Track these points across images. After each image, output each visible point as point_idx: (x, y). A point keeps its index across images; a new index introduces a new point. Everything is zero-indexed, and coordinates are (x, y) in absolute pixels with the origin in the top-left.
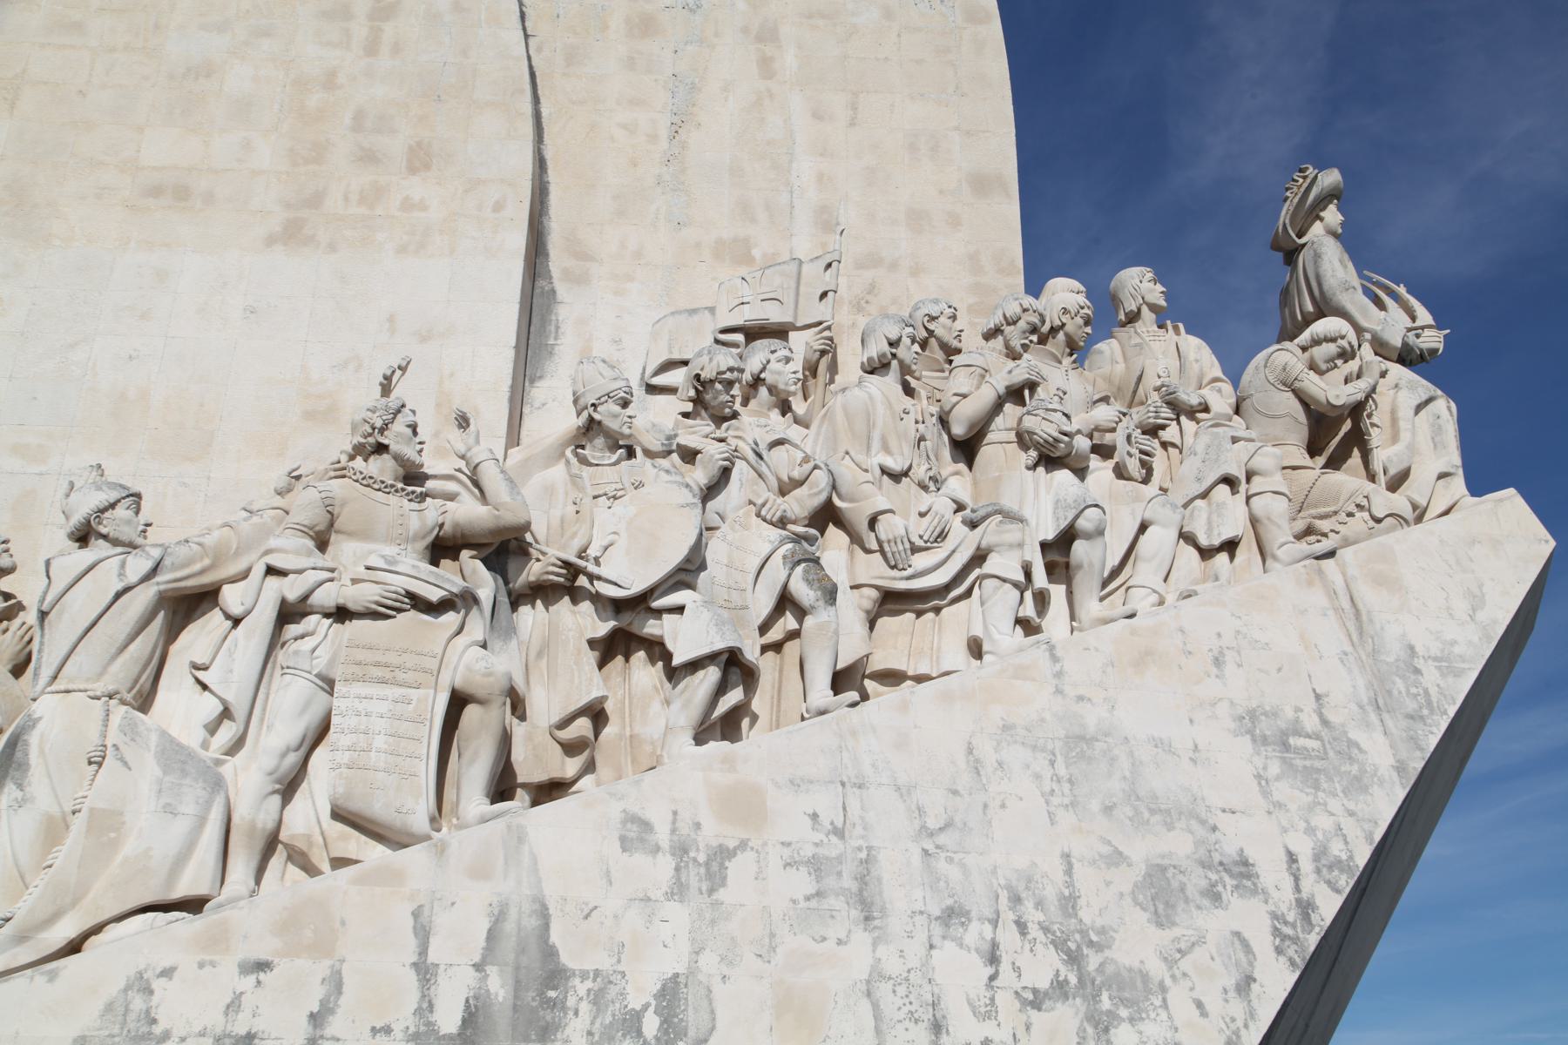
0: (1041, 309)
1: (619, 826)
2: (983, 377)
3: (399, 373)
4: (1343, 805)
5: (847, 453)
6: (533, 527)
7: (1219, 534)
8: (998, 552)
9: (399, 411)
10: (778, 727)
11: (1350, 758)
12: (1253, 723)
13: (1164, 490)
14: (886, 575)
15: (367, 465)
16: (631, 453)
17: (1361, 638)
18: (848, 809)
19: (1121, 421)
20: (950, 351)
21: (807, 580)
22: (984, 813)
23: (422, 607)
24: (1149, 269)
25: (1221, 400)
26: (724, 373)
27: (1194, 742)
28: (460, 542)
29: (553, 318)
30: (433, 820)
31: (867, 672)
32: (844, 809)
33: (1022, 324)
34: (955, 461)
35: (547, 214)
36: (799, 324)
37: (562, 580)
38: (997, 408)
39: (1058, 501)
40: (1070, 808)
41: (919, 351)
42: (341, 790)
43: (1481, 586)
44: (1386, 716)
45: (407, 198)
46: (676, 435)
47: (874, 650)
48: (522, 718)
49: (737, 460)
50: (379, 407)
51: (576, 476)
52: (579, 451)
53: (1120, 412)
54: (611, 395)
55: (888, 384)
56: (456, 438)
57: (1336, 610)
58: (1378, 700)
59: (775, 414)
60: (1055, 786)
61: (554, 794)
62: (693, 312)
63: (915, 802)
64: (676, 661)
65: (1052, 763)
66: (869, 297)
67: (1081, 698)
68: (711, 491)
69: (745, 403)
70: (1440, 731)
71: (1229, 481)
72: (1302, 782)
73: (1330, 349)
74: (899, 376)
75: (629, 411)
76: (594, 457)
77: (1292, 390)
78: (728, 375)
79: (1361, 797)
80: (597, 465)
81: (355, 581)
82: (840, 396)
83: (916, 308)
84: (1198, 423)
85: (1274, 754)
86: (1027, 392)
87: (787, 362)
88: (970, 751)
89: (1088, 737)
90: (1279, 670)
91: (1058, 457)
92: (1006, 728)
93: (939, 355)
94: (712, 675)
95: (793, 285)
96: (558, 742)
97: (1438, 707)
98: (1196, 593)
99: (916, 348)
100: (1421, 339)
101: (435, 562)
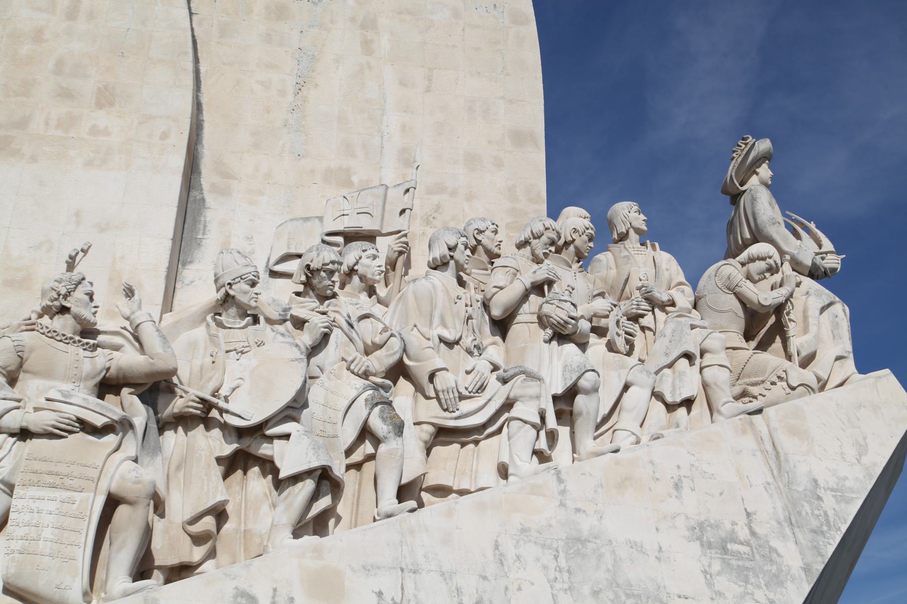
0: (558, 228)
1: (232, 599)
2: (515, 275)
3: (81, 254)
4: (765, 595)
5: (415, 326)
6: (179, 372)
7: (680, 394)
8: (520, 401)
9: (80, 283)
10: (356, 526)
11: (771, 560)
12: (702, 532)
13: (642, 361)
14: (439, 415)
15: (52, 322)
16: (256, 320)
17: (780, 473)
18: (405, 589)
19: (612, 310)
20: (493, 256)
21: (382, 417)
22: (506, 594)
23: (89, 430)
24: (635, 204)
25: (684, 298)
26: (328, 264)
27: (659, 544)
28: (122, 381)
29: (202, 219)
30: (85, 594)
31: (424, 486)
32: (402, 588)
33: (544, 239)
34: (493, 334)
35: (201, 143)
36: (384, 232)
37: (199, 412)
38: (525, 297)
39: (566, 366)
40: (568, 592)
41: (470, 255)
42: (12, 571)
43: (865, 438)
44: (796, 530)
45: (94, 126)
46: (290, 309)
47: (429, 471)
48: (162, 516)
49: (335, 328)
50: (64, 279)
51: (214, 335)
52: (217, 317)
53: (612, 304)
54: (243, 277)
55: (447, 277)
56: (124, 305)
57: (761, 451)
58: (791, 518)
59: (364, 296)
60: (558, 575)
61: (183, 574)
62: (307, 219)
63: (454, 585)
64: (282, 475)
65: (556, 558)
66: (435, 215)
67: (578, 510)
68: (314, 350)
69: (342, 287)
70: (835, 542)
71: (688, 356)
72: (736, 577)
73: (762, 265)
74: (455, 272)
75: (256, 289)
76: (228, 322)
77: (735, 294)
78: (330, 266)
79: (779, 590)
80: (230, 328)
81: (36, 409)
82: (411, 285)
83: (469, 224)
84: (667, 314)
85: (716, 555)
86: (546, 287)
87: (374, 259)
88: (497, 547)
89: (583, 539)
90: (721, 494)
91: (567, 335)
92: (524, 530)
93: (485, 258)
94: (308, 486)
95: (380, 203)
96: (189, 535)
97: (834, 525)
98: (663, 437)
99: (468, 252)
100: (825, 261)
101: (101, 396)
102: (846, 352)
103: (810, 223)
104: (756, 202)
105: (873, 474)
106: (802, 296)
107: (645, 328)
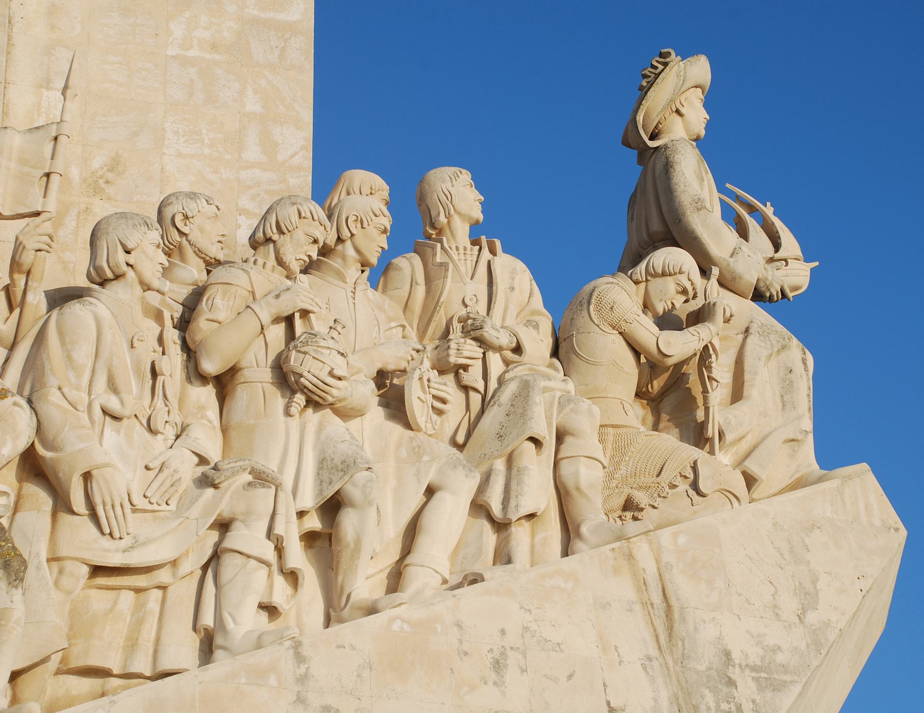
7: (517, 506)
43: (815, 581)
57: (643, 604)
90: (570, 677)
98: (483, 580)
102: (801, 433)
103: (766, 206)
104: (672, 171)
105: (822, 640)
106: (737, 334)
107: (469, 390)
